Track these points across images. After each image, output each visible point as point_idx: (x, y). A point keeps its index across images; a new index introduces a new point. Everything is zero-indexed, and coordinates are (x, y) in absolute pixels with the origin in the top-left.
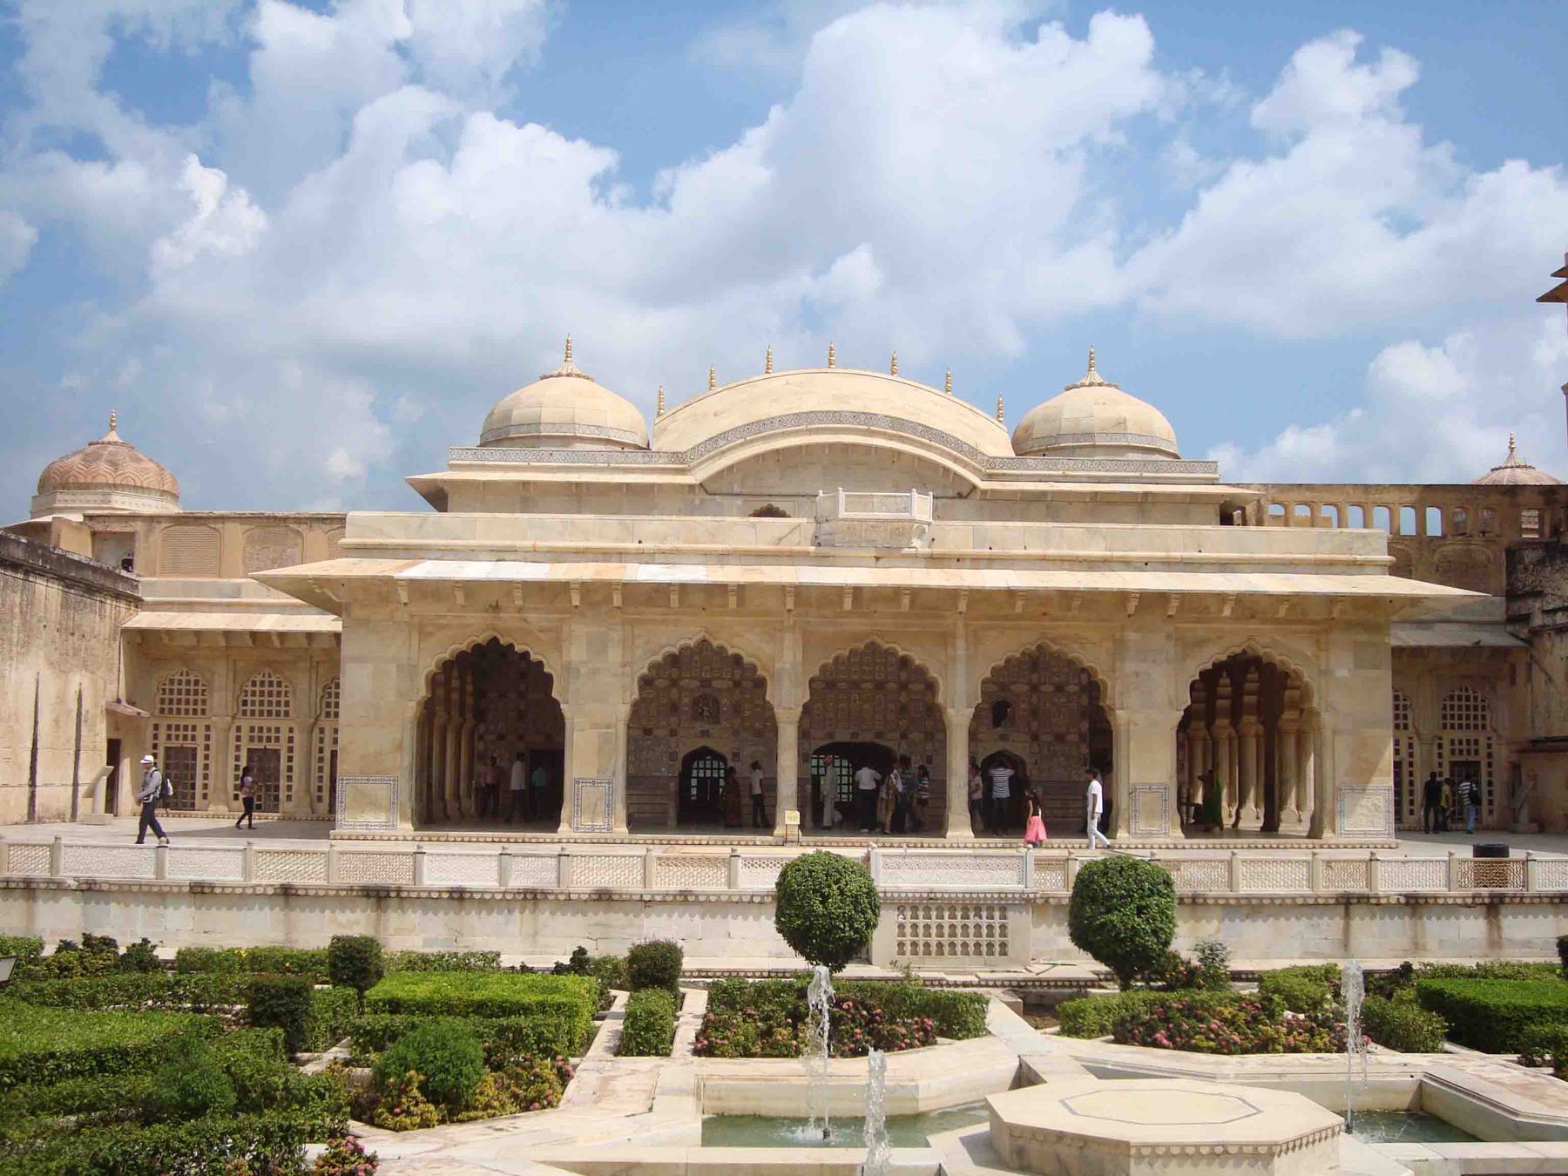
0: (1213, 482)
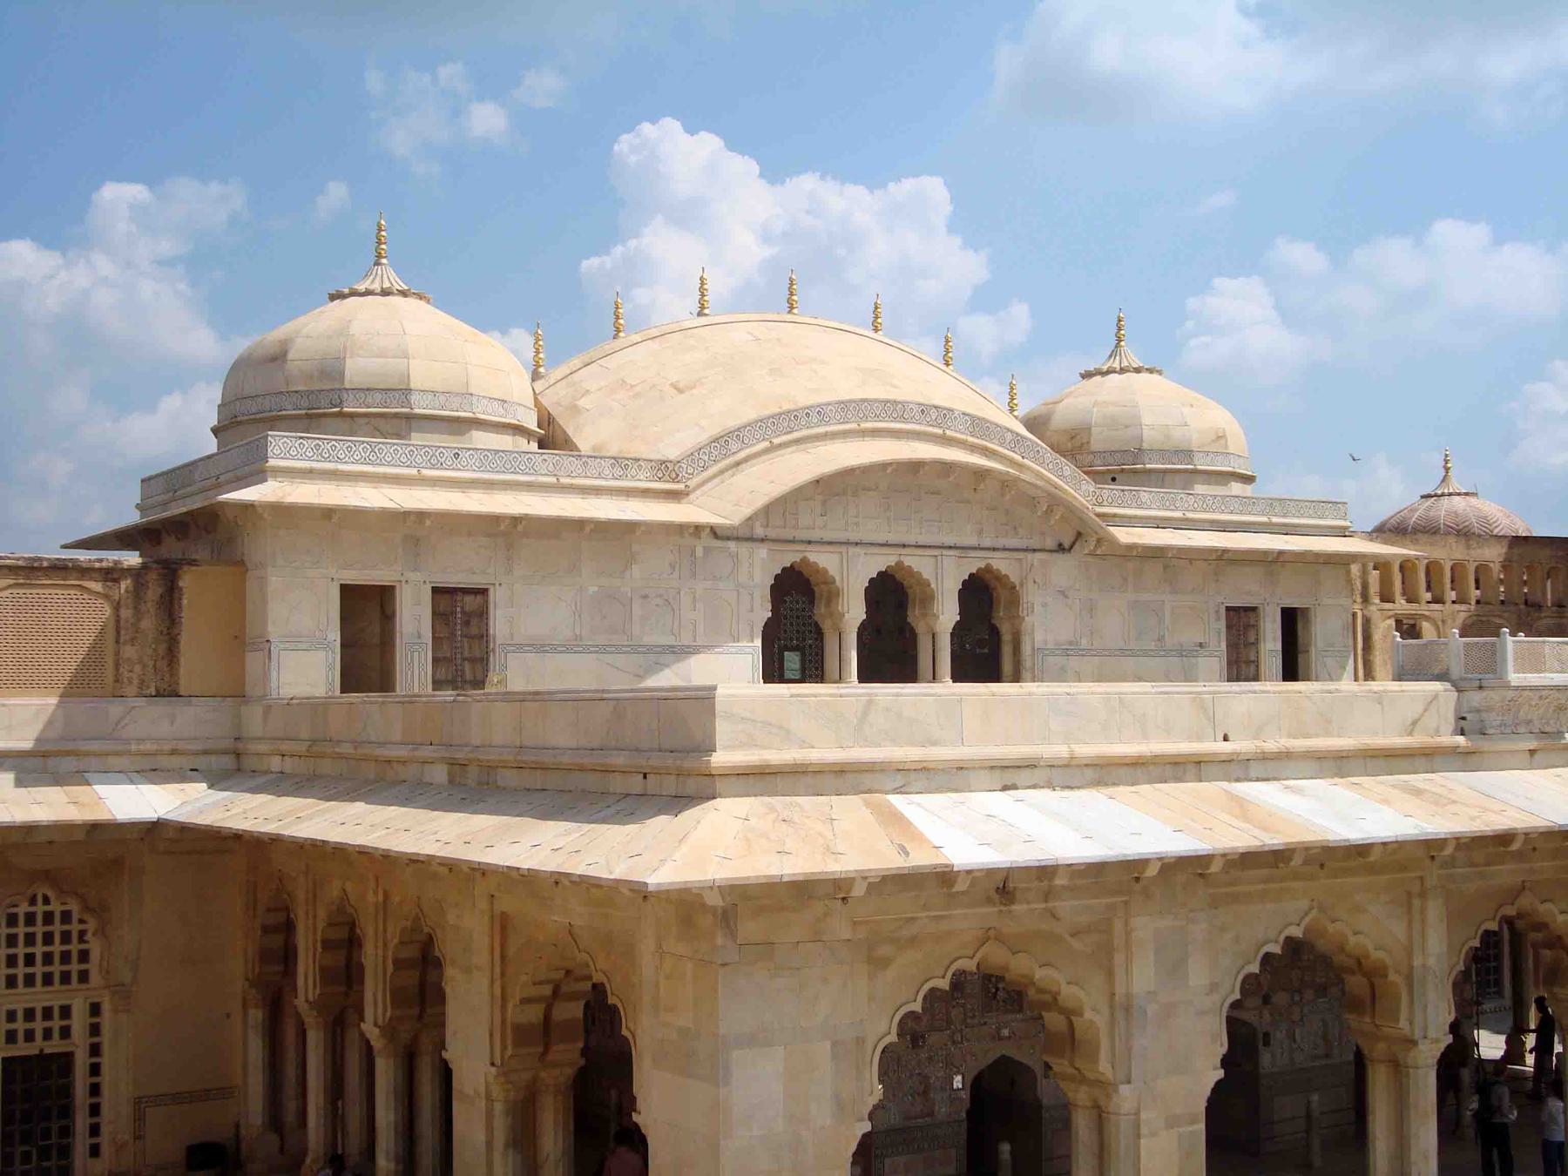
0: (1343, 533)
